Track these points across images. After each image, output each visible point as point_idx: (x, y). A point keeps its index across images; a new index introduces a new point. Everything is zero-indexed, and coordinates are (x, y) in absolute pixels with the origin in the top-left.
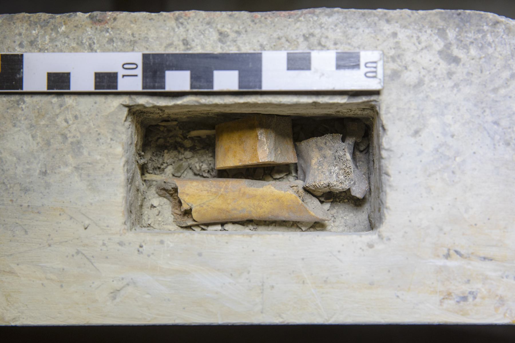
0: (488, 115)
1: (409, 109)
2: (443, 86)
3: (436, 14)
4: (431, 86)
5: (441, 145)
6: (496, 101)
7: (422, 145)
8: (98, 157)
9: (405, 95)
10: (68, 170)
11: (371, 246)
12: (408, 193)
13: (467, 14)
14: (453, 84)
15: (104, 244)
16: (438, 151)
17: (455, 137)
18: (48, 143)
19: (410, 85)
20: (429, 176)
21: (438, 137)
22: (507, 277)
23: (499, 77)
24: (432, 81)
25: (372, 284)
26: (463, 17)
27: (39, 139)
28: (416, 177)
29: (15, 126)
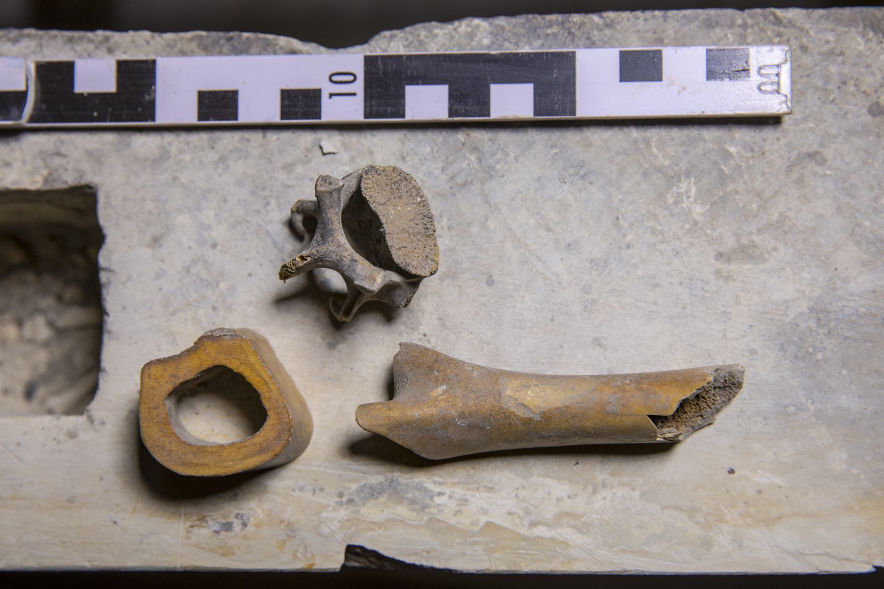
0: (273, 210)
1: (144, 199)
2: (201, 161)
3: (191, 40)
4: (181, 161)
5: (194, 262)
6: (288, 187)
7: (163, 261)
9: (137, 176)
12: (136, 343)
13: (244, 39)
14: (216, 157)
16: (189, 272)
17: (219, 248)
19: (146, 160)
20: (173, 314)
21: (190, 248)
22: (301, 489)
23: (294, 146)
24: (181, 151)
25: (71, 501)
26: (236, 44)
28: (151, 316)
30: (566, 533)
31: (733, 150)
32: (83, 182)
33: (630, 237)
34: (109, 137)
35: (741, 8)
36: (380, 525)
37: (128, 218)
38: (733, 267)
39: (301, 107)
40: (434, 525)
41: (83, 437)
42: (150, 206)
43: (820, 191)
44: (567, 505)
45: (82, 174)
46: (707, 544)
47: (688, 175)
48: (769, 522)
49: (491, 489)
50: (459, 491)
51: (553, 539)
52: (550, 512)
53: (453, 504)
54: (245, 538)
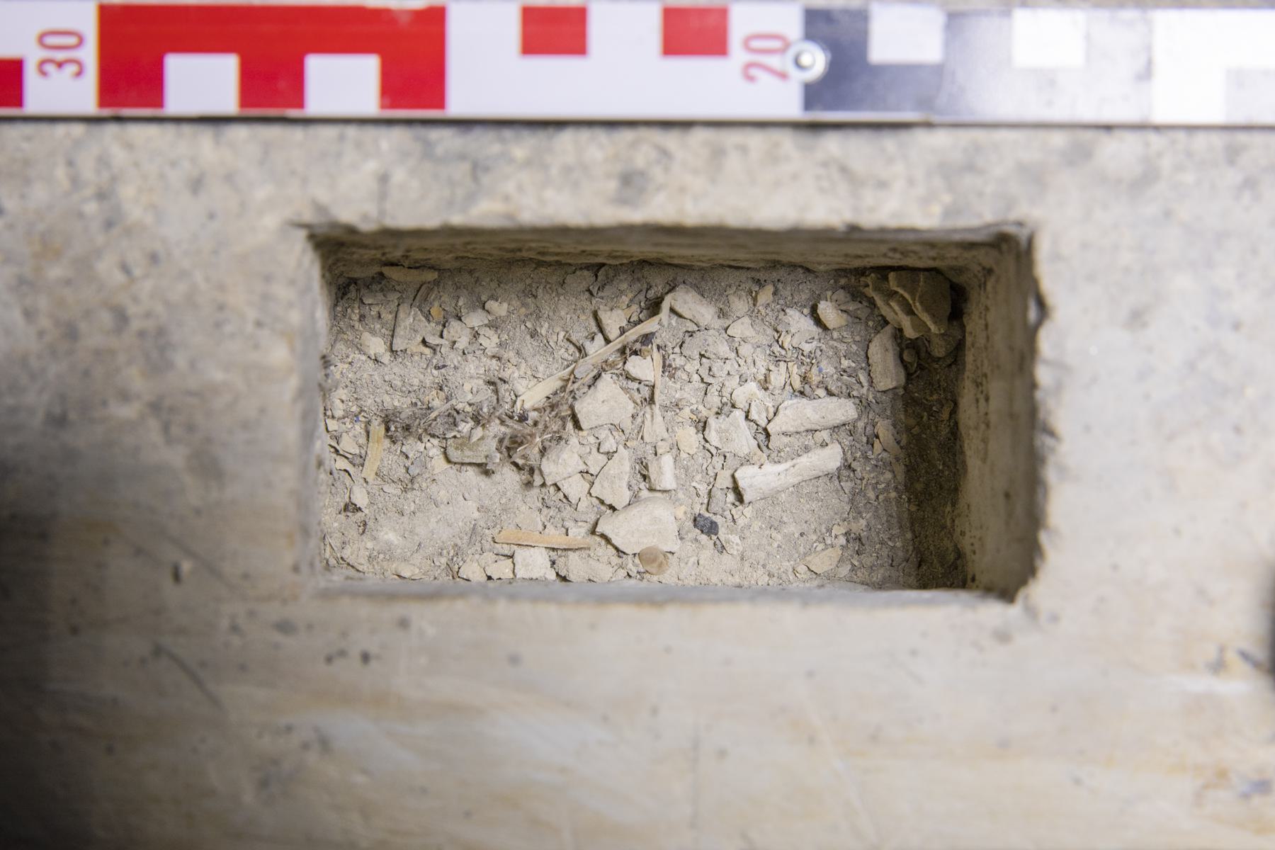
8: (218, 376)
11: (1003, 637)
15: (235, 629)
25: (1004, 744)
27: (45, 322)
32: (1014, 216)
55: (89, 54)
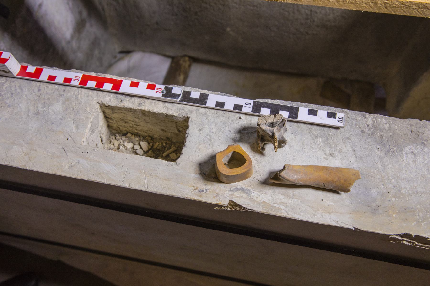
10: (70, 120)
11: (172, 165)
15: (73, 147)
18: (67, 110)
24: (209, 113)
29: (57, 102)
30: (282, 207)
31: (330, 134)
33: (305, 147)
34: (194, 108)
35: (335, 108)
36: (238, 197)
37: (195, 124)
38: (328, 157)
39: (238, 107)
40: (251, 200)
41: (174, 166)
42: (200, 123)
43: (349, 145)
44: (283, 200)
45: (187, 114)
46: (314, 215)
47: (320, 137)
48: (330, 213)
49: (266, 194)
50: (258, 193)
51: (278, 207)
52: (278, 202)
53: (256, 196)
54: (206, 194)
55: (80, 79)
